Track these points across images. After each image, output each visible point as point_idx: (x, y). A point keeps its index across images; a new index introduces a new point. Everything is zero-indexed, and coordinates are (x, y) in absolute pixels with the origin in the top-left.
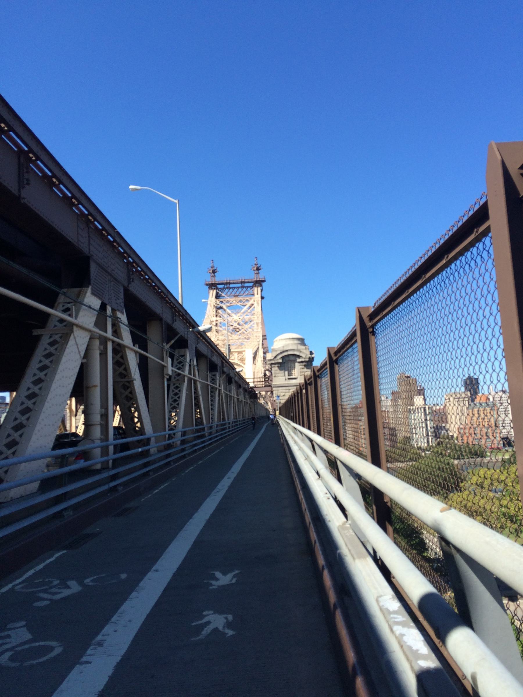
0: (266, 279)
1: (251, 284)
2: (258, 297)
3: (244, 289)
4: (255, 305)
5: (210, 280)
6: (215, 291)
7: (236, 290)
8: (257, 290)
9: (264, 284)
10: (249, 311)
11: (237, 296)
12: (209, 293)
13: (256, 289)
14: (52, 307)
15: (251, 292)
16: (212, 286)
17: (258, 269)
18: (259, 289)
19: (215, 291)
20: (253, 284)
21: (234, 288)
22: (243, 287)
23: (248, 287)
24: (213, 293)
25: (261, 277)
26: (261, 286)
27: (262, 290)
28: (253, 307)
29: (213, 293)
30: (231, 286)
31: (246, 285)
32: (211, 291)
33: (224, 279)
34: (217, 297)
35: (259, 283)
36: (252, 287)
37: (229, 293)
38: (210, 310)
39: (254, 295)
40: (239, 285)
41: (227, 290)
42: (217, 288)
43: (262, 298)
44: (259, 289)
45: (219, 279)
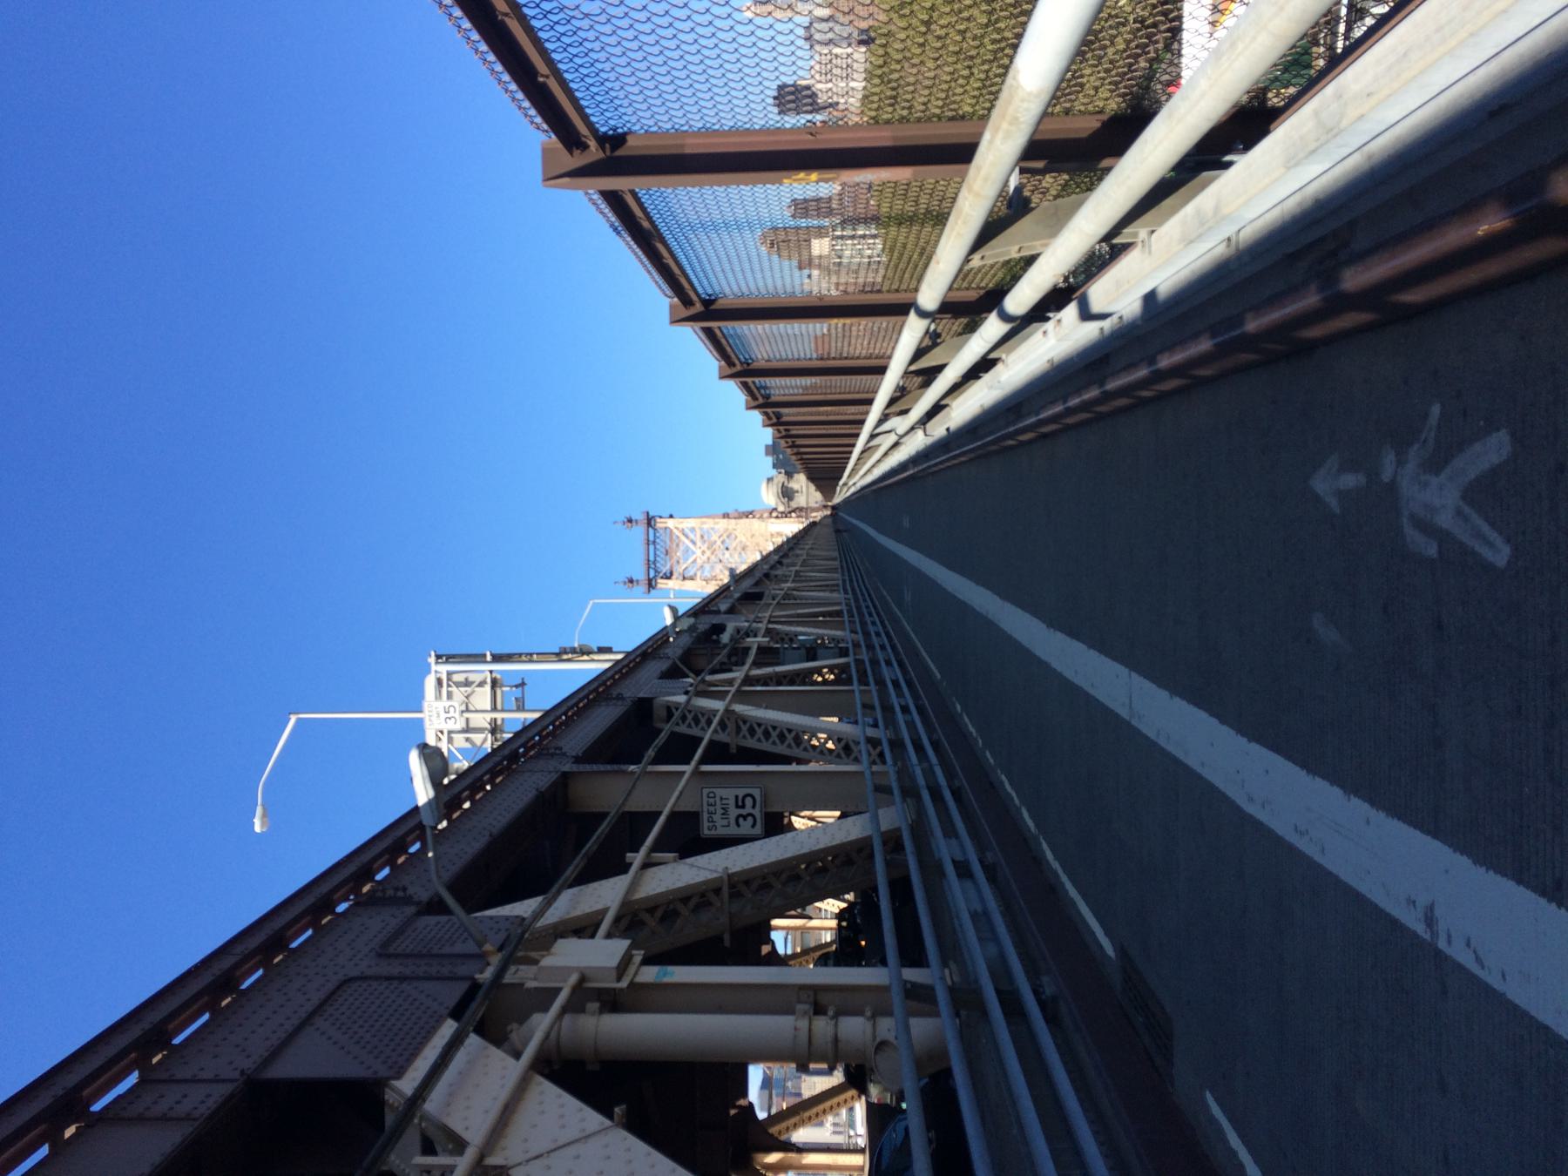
0: (645, 510)
1: (651, 530)
2: (671, 523)
3: (658, 540)
4: (680, 526)
5: (643, 588)
6: (659, 581)
7: (658, 553)
8: (660, 524)
9: (651, 514)
10: (692, 536)
11: (667, 551)
12: (661, 589)
13: (658, 525)
14: (700, 740)
15: (661, 531)
16: (651, 584)
17: (630, 521)
18: (658, 520)
19: (659, 581)
20: (651, 530)
21: (655, 554)
22: (654, 542)
23: (655, 536)
24: (662, 584)
25: (641, 517)
26: (653, 517)
27: (661, 517)
28: (687, 531)
29: (662, 584)
30: (652, 558)
31: (651, 538)
32: (659, 586)
33: (643, 568)
34: (669, 576)
35: (650, 521)
36: (655, 529)
37: (662, 562)
38: (689, 586)
39: (666, 528)
40: (652, 547)
41: (658, 565)
42: (655, 576)
43: (671, 516)
44: (658, 520)
45: (640, 574)
